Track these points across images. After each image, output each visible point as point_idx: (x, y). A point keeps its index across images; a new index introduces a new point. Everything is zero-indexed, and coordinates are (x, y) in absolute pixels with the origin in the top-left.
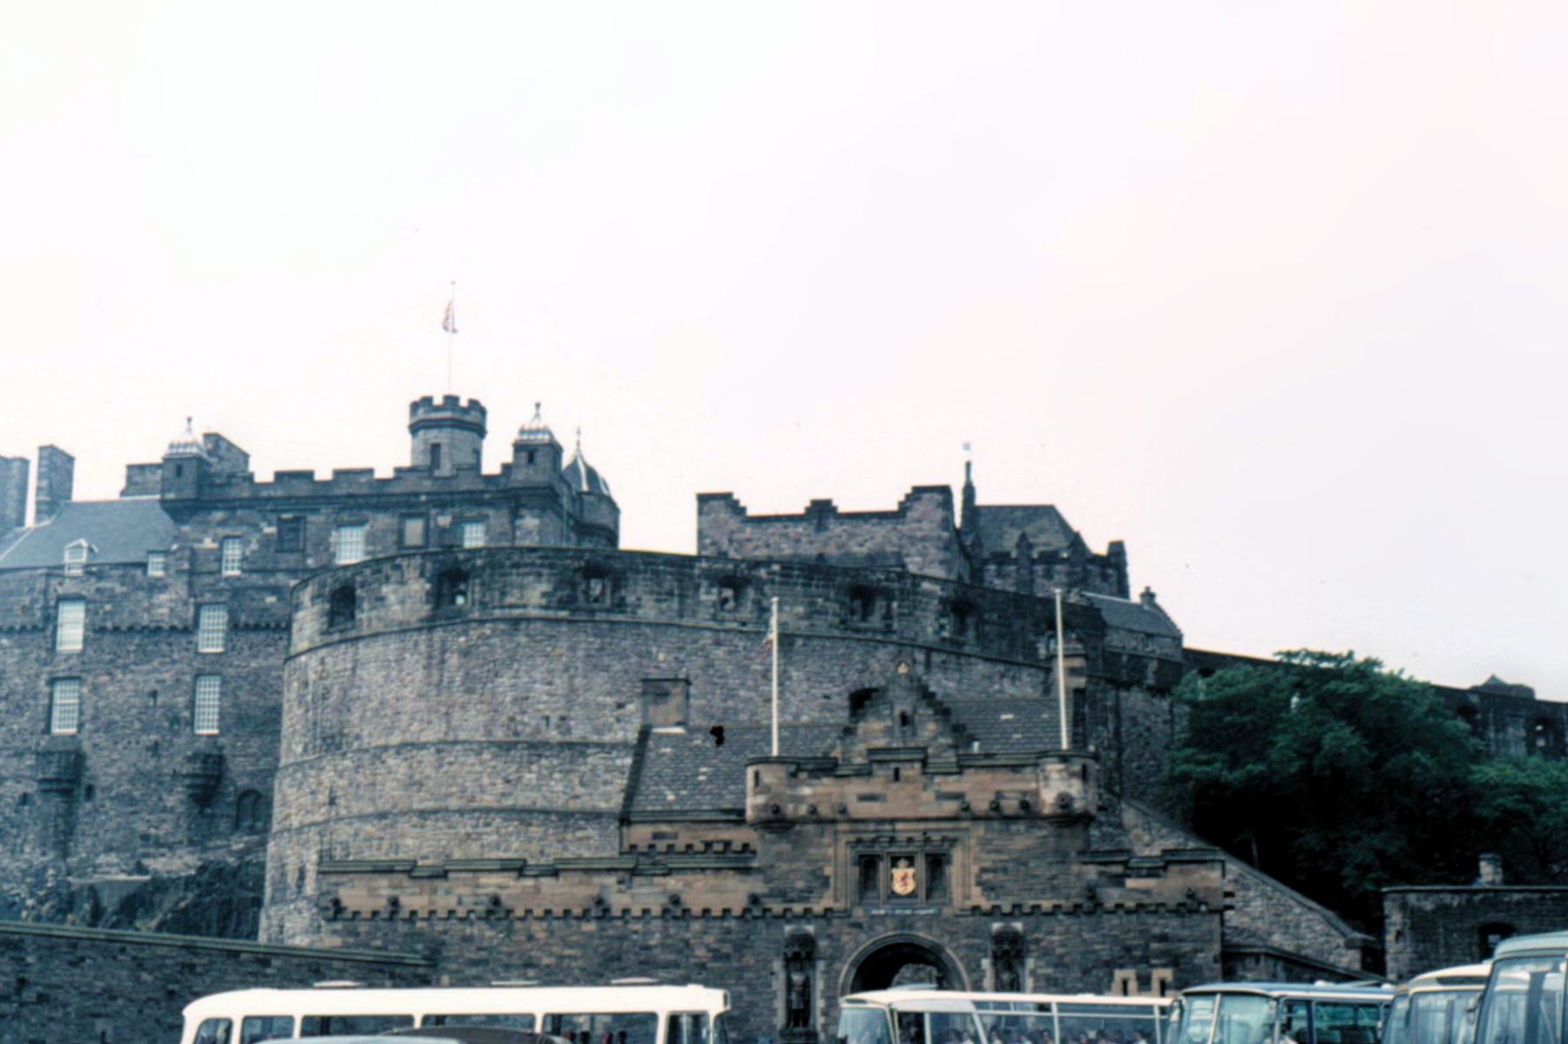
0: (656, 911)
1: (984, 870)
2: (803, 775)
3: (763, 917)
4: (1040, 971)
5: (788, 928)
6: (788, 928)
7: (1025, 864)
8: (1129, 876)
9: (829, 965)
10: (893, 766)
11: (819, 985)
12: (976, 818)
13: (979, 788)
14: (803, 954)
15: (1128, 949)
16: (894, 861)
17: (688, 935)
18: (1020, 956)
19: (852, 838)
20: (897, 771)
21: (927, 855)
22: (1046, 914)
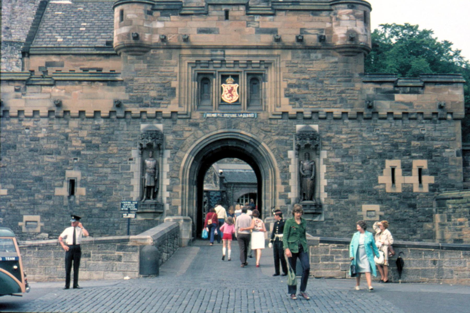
0: (44, 112)
1: (290, 86)
2: (157, 14)
3: (124, 118)
4: (331, 160)
5: (143, 126)
6: (143, 126)
7: (322, 82)
8: (397, 92)
9: (174, 154)
10: (224, 8)
11: (166, 168)
12: (286, 48)
13: (288, 26)
14: (155, 145)
15: (396, 145)
16: (224, 78)
17: (67, 130)
18: (317, 149)
19: (193, 60)
20: (227, 12)
21: (248, 74)
22: (335, 119)
